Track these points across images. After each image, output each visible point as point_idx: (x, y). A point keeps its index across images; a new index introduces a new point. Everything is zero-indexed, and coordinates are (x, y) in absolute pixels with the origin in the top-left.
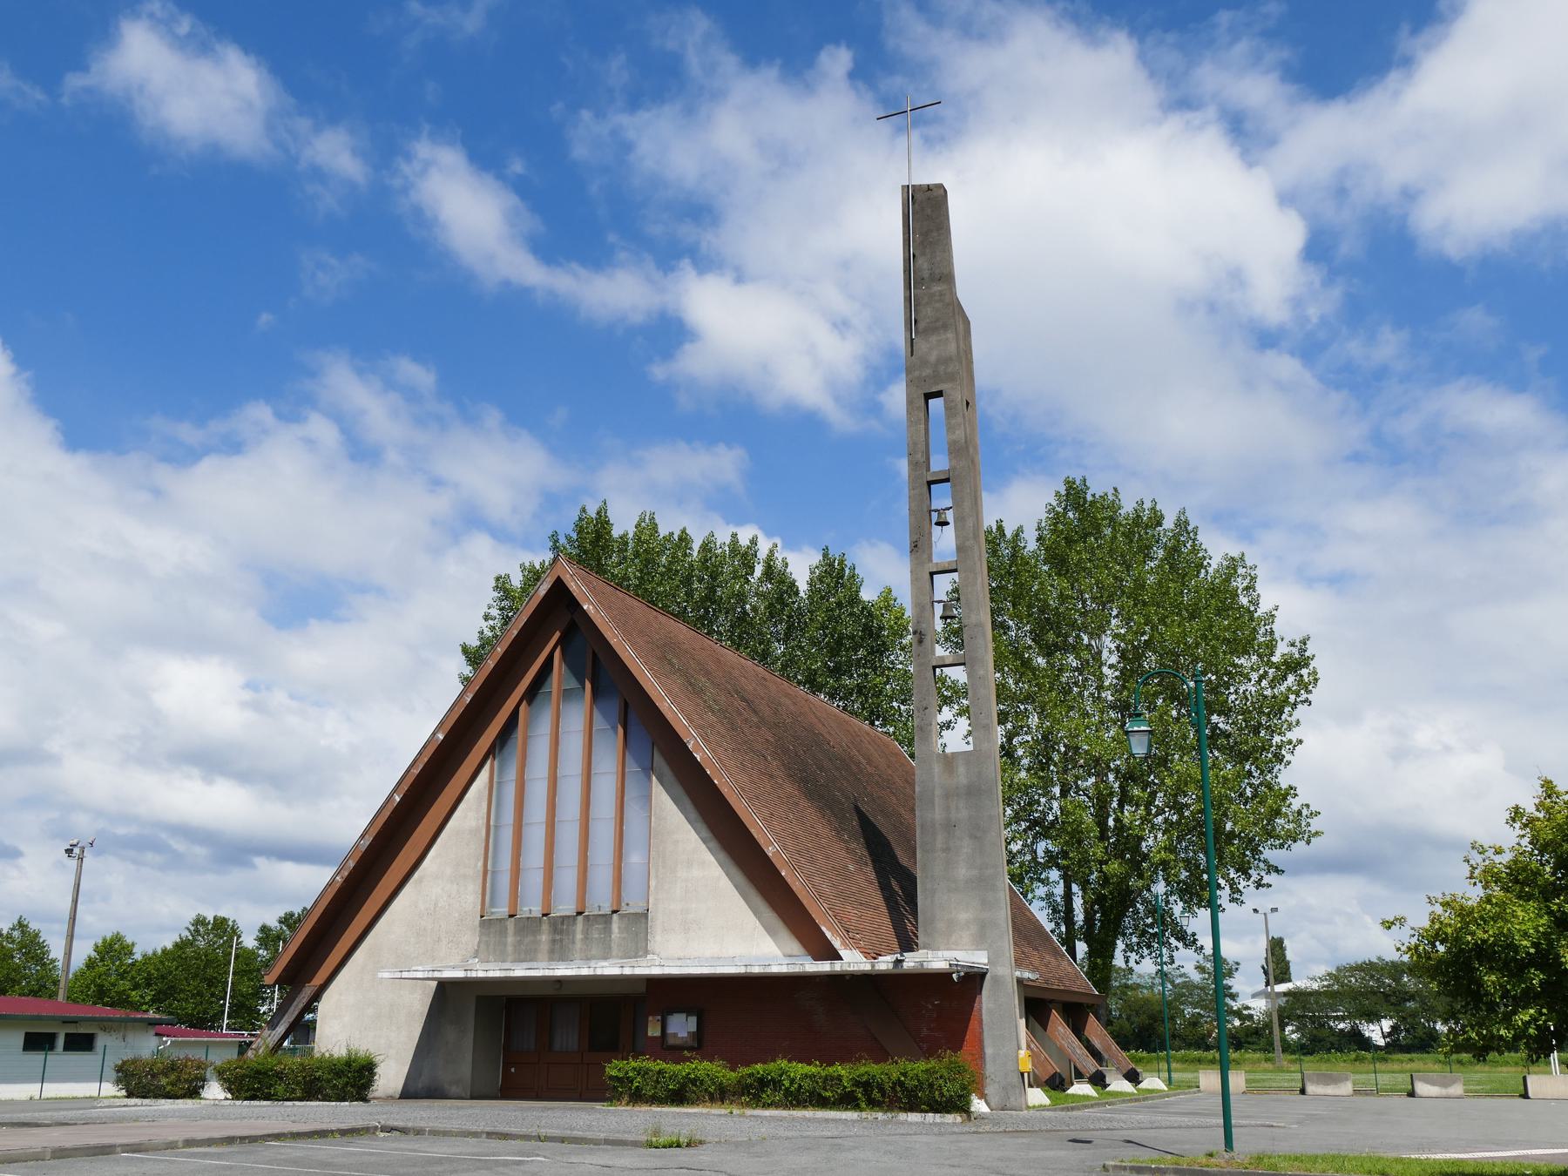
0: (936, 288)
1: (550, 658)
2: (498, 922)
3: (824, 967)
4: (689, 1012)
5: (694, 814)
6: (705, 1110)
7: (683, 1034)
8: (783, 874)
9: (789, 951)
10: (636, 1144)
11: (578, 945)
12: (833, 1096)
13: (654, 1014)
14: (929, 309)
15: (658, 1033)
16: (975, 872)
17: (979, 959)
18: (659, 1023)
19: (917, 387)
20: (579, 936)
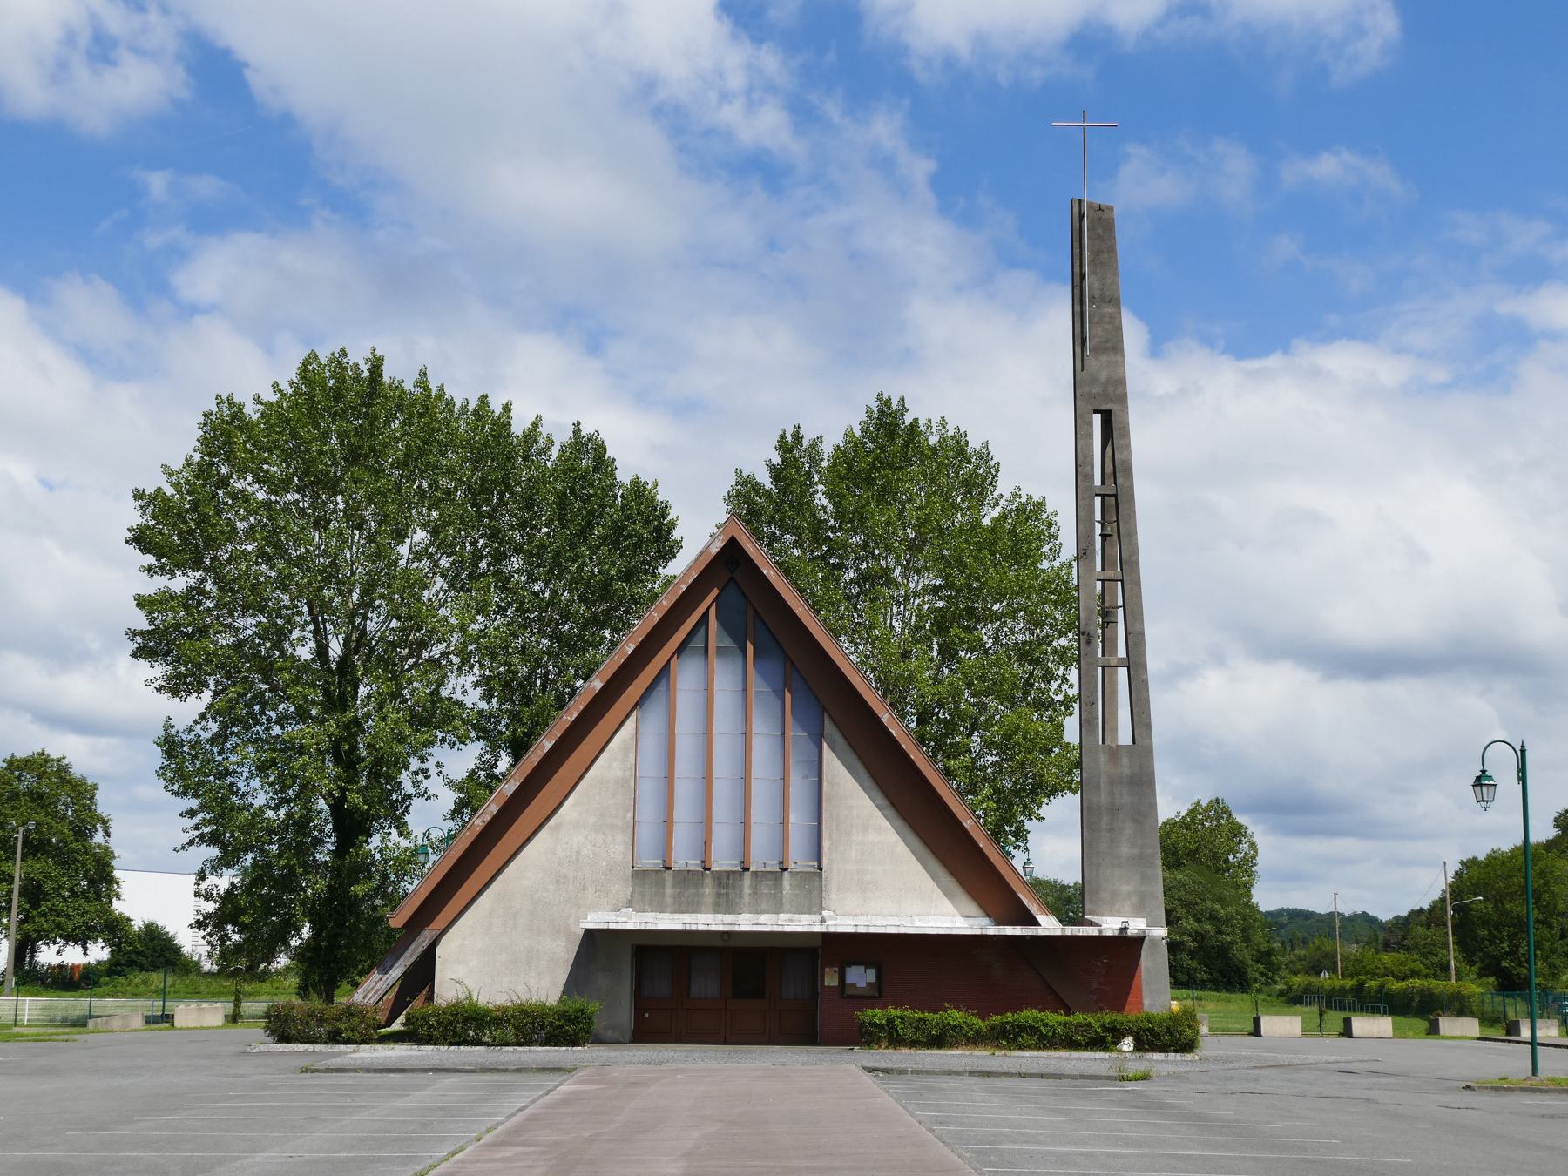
0: (1107, 310)
1: (707, 612)
2: (654, 874)
3: (1070, 931)
4: (868, 965)
5: (869, 782)
6: (962, 1052)
7: (862, 984)
8: (981, 846)
9: (967, 913)
10: (1108, 1078)
11: (746, 899)
12: (1084, 1040)
13: (831, 966)
14: (1099, 329)
15: (835, 983)
16: (1136, 851)
17: (1137, 925)
18: (837, 974)
19: (1088, 402)
20: (747, 891)
